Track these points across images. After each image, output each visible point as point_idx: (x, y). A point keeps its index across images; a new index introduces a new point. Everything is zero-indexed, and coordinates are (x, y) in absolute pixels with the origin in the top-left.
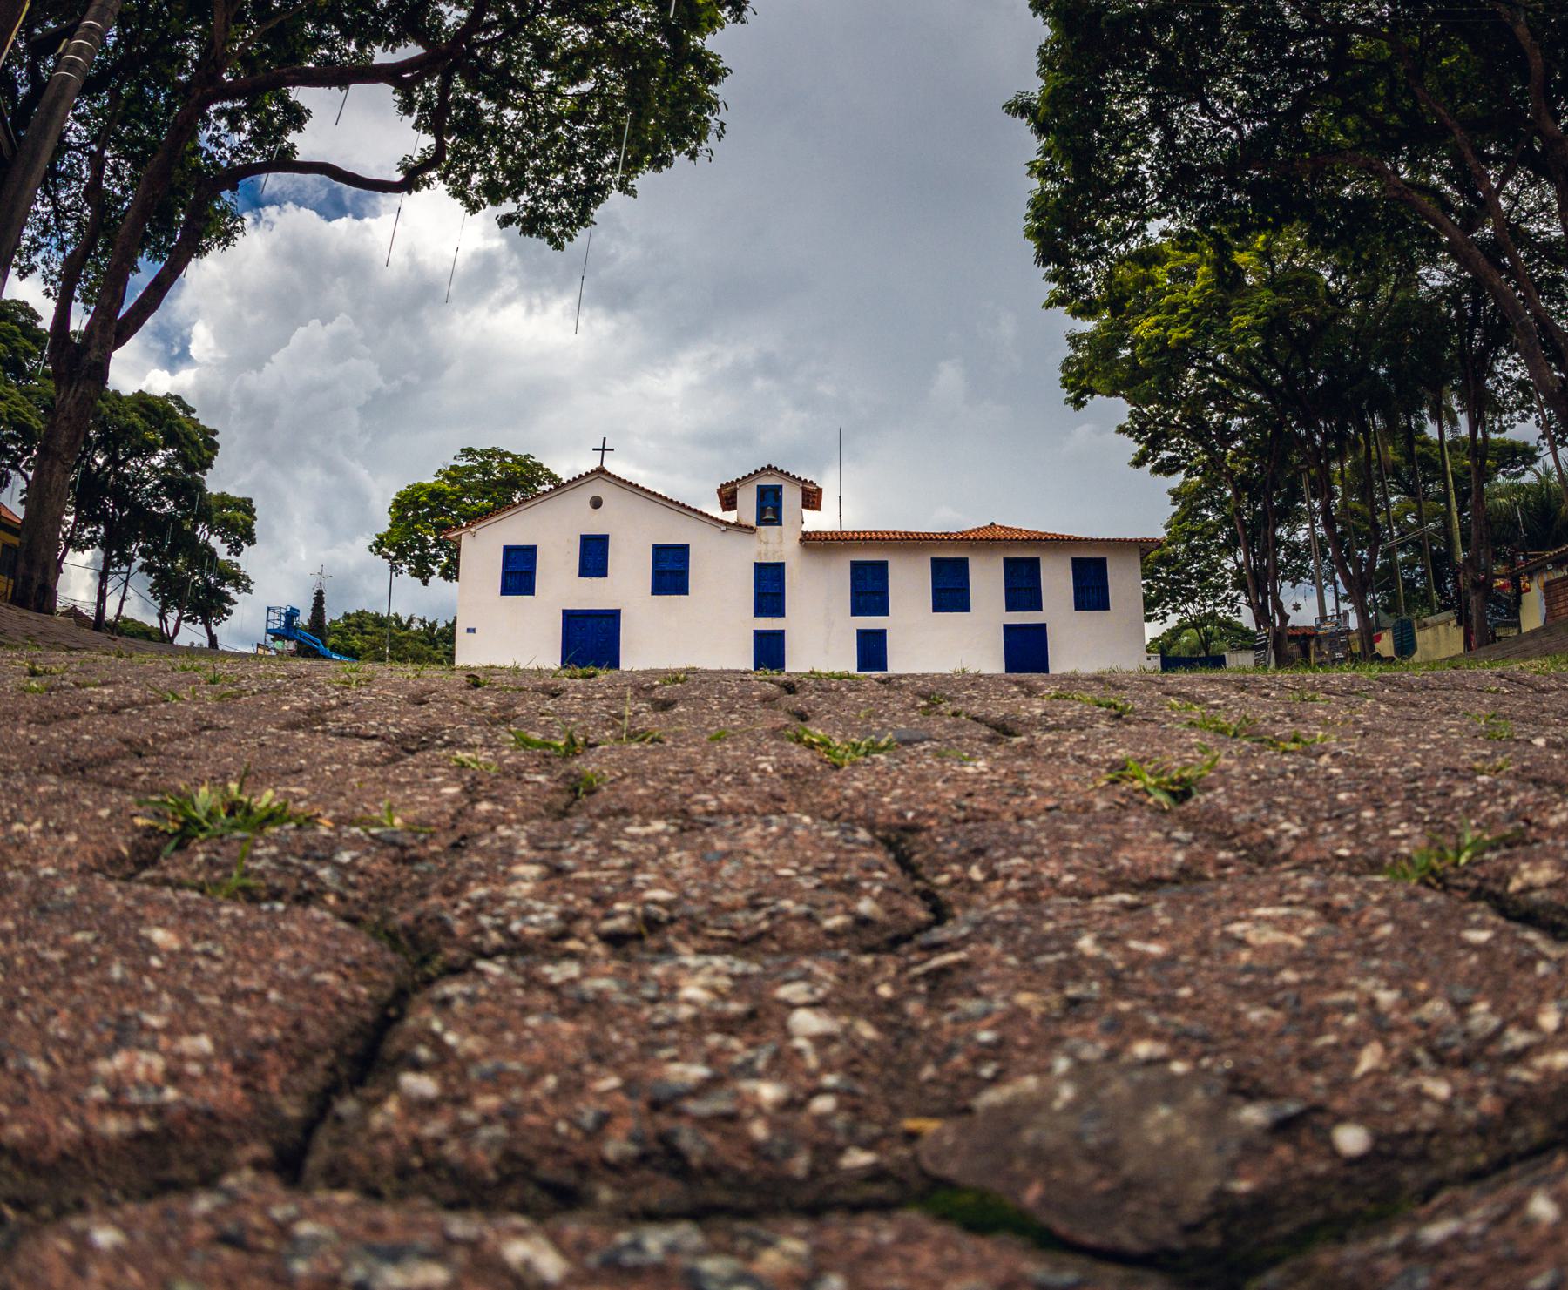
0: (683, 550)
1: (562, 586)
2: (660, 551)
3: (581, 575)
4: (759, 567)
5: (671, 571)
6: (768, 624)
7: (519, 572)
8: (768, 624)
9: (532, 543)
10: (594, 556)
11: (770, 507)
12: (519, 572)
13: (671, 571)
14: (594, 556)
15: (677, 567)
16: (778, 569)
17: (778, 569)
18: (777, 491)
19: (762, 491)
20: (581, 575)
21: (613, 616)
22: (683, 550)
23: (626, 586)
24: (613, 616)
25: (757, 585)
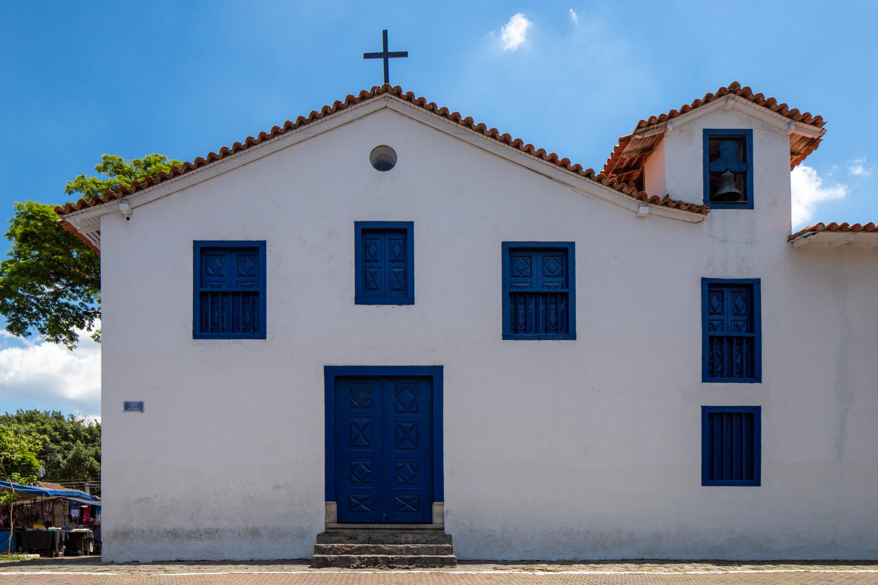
0: (562, 254)
1: (318, 321)
2: (516, 254)
3: (359, 300)
4: (714, 290)
5: (538, 294)
6: (731, 394)
7: (230, 293)
8: (731, 394)
9: (253, 236)
10: (384, 262)
11: (730, 174)
12: (230, 293)
13: (538, 294)
14: (384, 262)
15: (554, 285)
16: (748, 290)
17: (748, 290)
18: (742, 141)
19: (715, 142)
20: (359, 300)
21: (428, 380)
22: (562, 254)
23: (449, 324)
24: (428, 380)
25: (708, 325)
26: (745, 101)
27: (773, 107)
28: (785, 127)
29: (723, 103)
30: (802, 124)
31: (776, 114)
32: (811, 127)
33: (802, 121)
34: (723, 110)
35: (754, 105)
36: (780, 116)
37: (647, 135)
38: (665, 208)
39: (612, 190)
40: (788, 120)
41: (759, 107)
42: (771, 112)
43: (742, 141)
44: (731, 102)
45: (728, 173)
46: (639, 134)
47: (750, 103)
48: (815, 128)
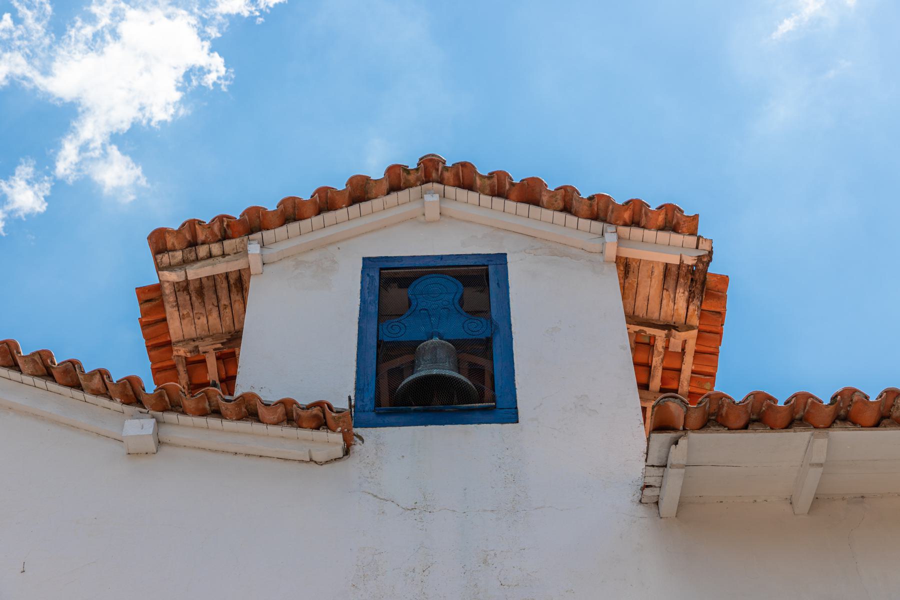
18: (478, 281)
26: (473, 196)
27: (545, 199)
28: (596, 245)
29: (415, 206)
30: (636, 232)
31: (560, 216)
32: (664, 236)
33: (635, 223)
34: (418, 220)
35: (498, 202)
36: (571, 219)
37: (195, 272)
38: (214, 422)
39: (51, 386)
40: (597, 226)
41: (510, 205)
42: (548, 214)
43: (478, 281)
44: (432, 199)
45: (436, 340)
46: (170, 267)
47: (486, 199)
48: (677, 238)
